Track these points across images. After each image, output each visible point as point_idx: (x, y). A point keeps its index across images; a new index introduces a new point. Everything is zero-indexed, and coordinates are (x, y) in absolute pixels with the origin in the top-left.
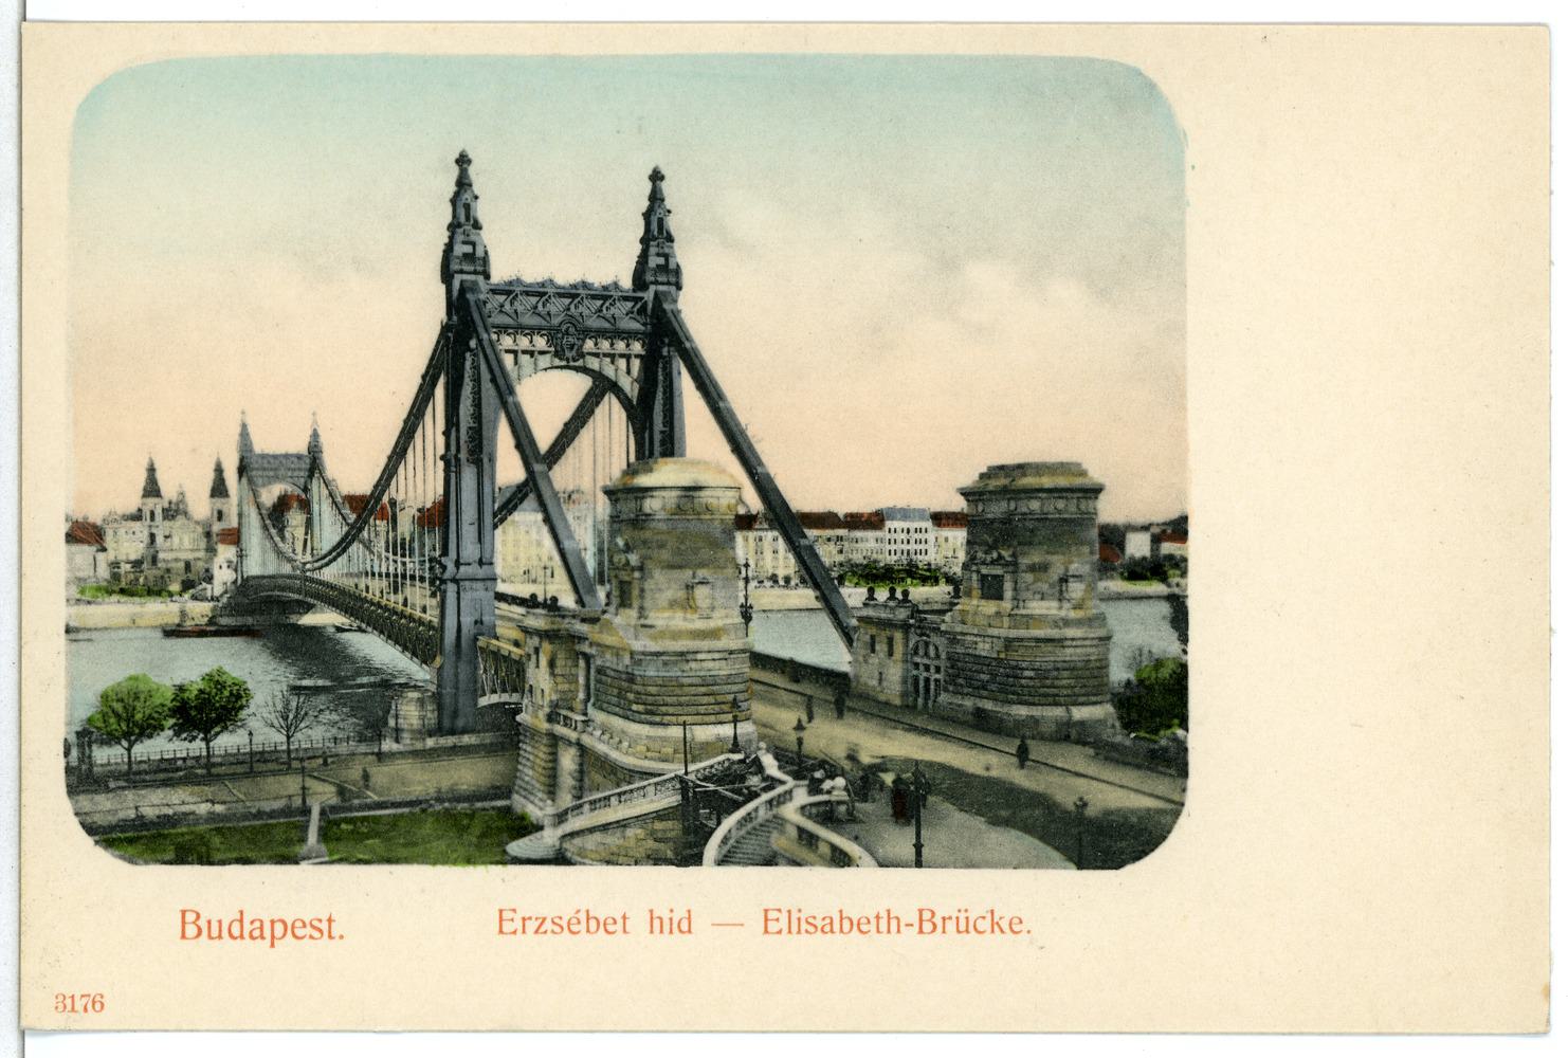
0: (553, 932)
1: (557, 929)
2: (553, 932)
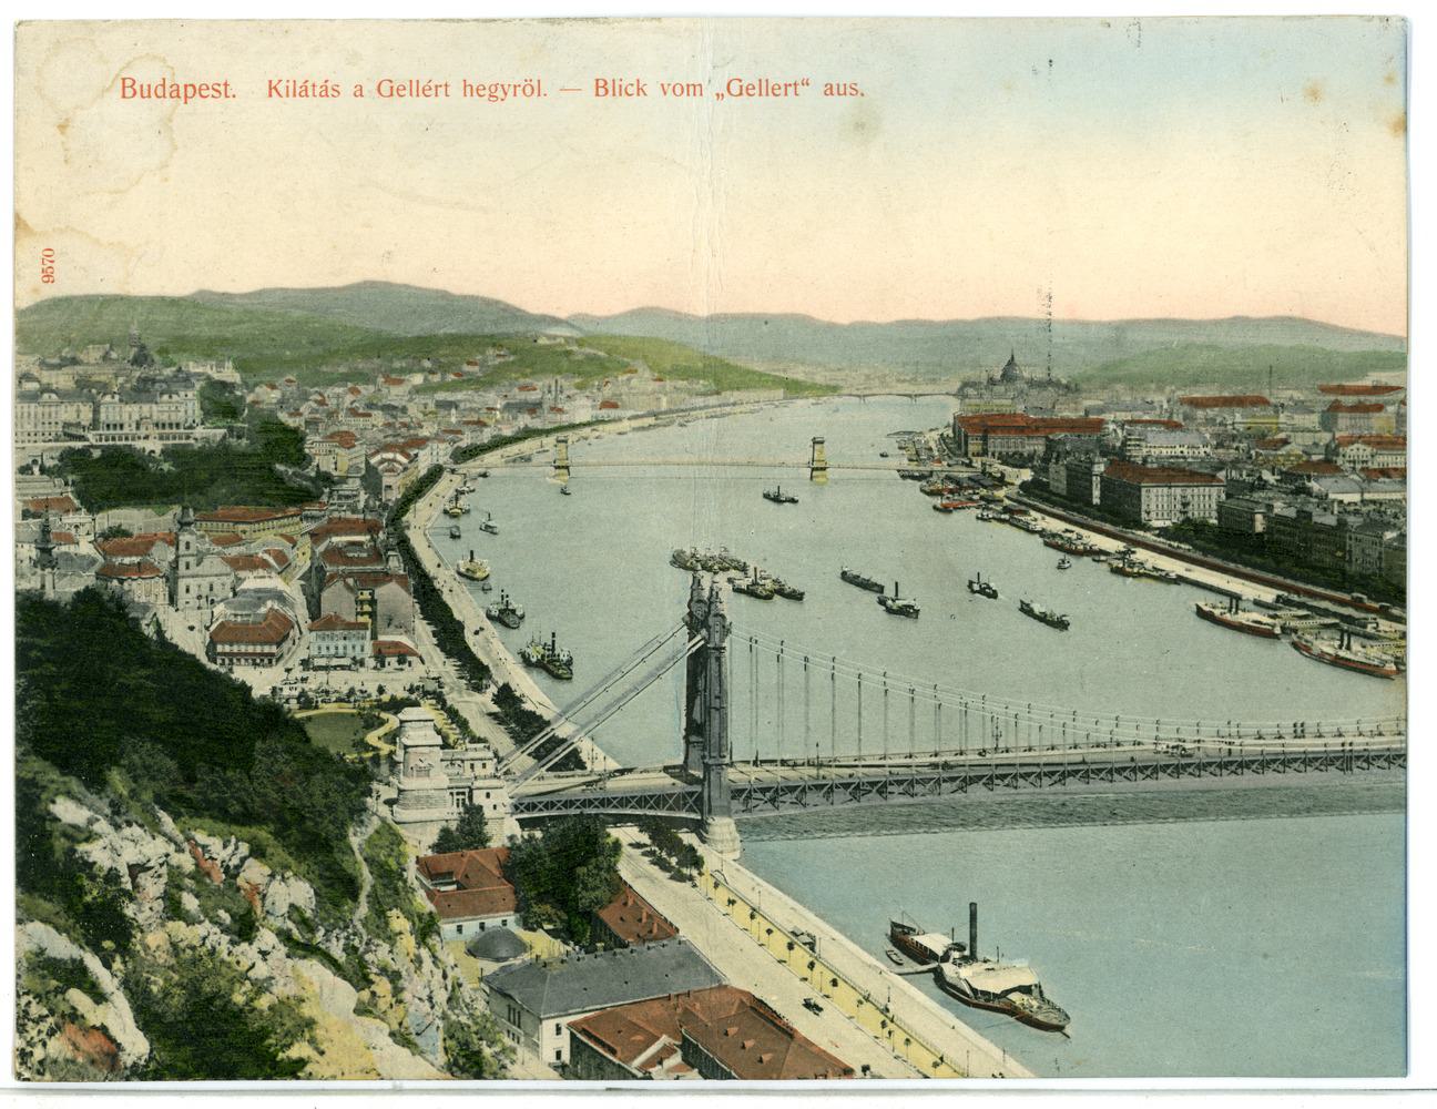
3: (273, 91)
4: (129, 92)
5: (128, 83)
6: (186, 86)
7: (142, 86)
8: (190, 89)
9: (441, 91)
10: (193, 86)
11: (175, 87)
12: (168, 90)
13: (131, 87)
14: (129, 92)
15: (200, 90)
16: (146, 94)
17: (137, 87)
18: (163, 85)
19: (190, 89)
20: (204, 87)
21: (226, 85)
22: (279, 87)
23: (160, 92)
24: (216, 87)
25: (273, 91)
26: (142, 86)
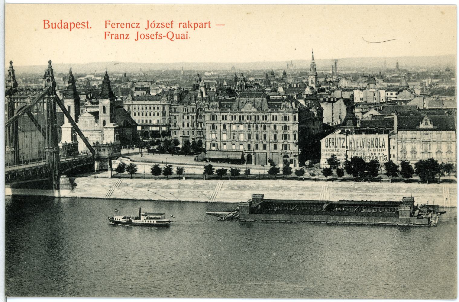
0: (162, 27)
1: (163, 26)
2: (162, 27)
3: (190, 26)
4: (47, 26)
5: (46, 22)
6: (71, 23)
7: (52, 23)
8: (72, 25)
9: (207, 25)
10: (74, 24)
11: (66, 24)
12: (63, 25)
13: (48, 24)
14: (47, 26)
15: (77, 25)
16: (54, 27)
17: (50, 24)
18: (61, 23)
19: (72, 25)
20: (78, 24)
21: (87, 23)
22: (191, 25)
23: (60, 26)
24: (83, 24)
25: (190, 26)
26: (52, 23)
